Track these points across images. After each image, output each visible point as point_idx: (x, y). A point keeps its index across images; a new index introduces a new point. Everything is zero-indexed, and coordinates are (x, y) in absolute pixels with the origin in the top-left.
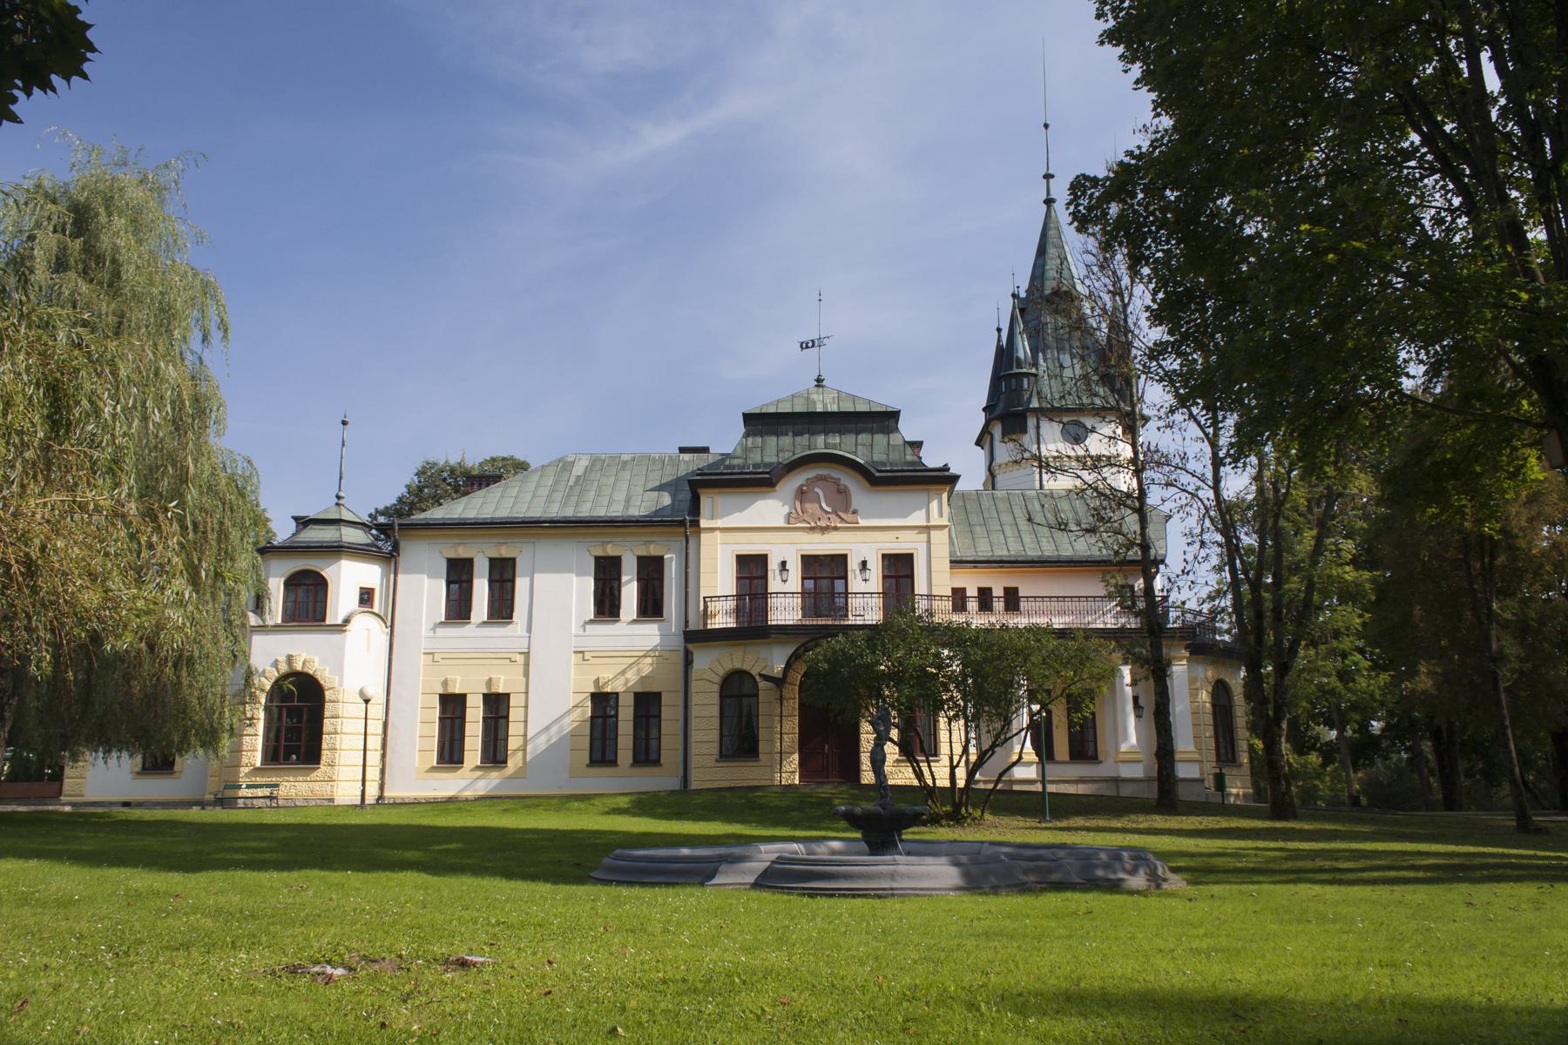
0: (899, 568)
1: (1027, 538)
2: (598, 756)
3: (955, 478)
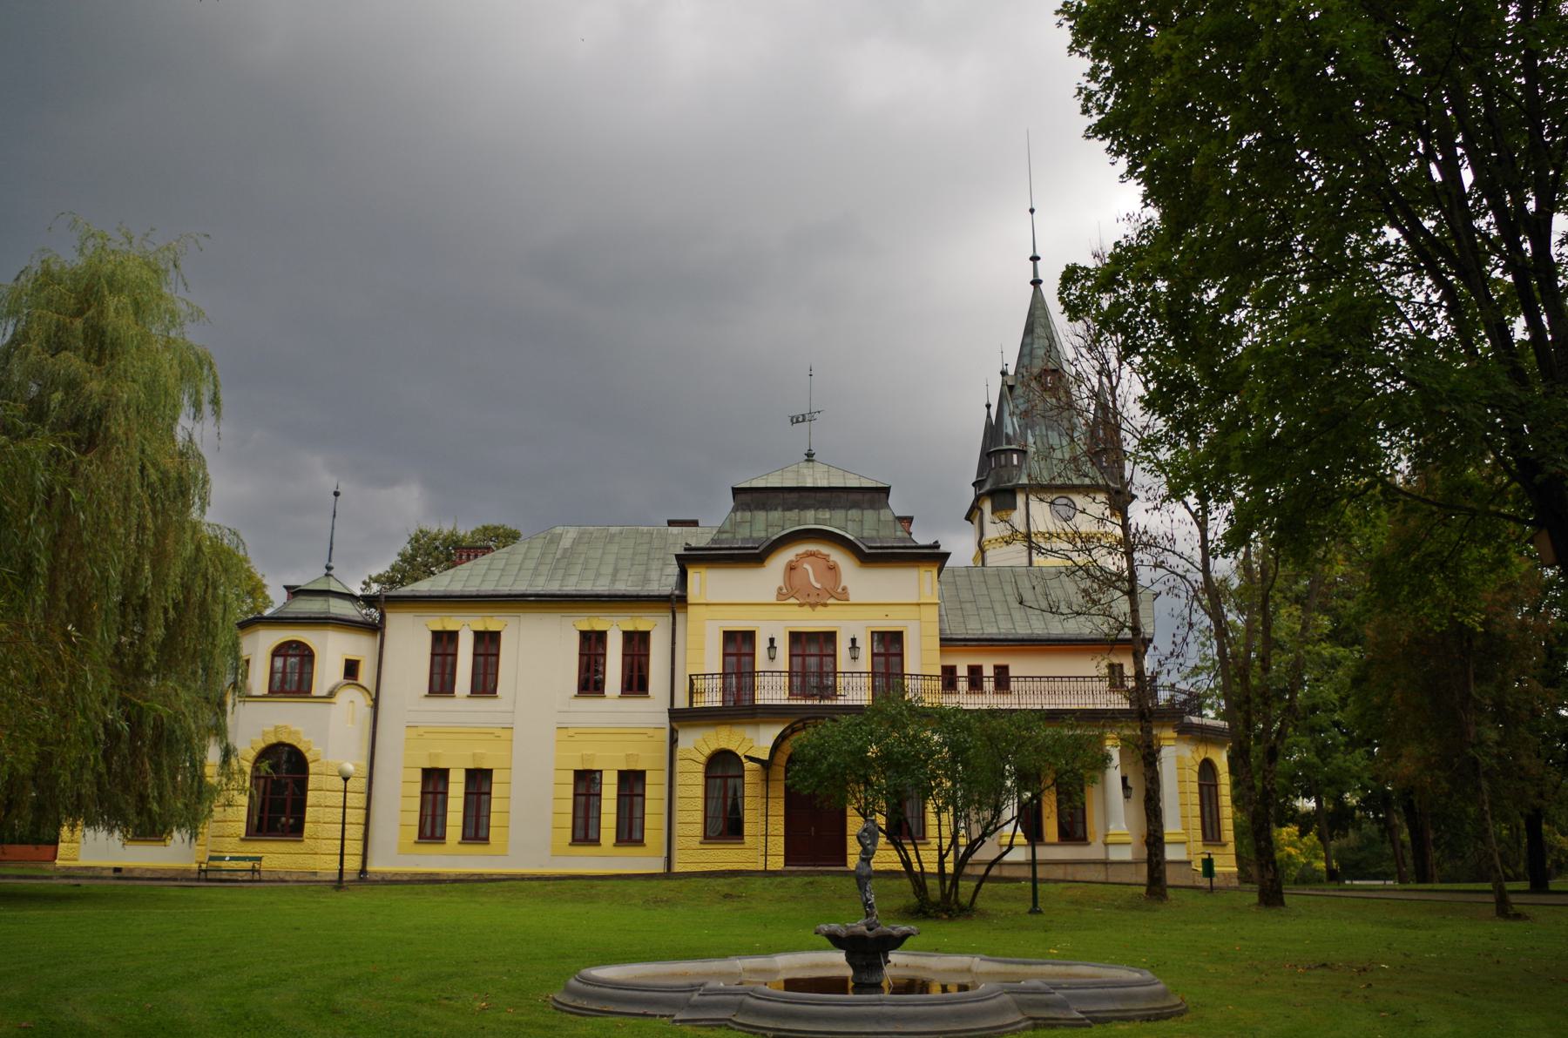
0: (889, 643)
2: (580, 834)
3: (947, 555)
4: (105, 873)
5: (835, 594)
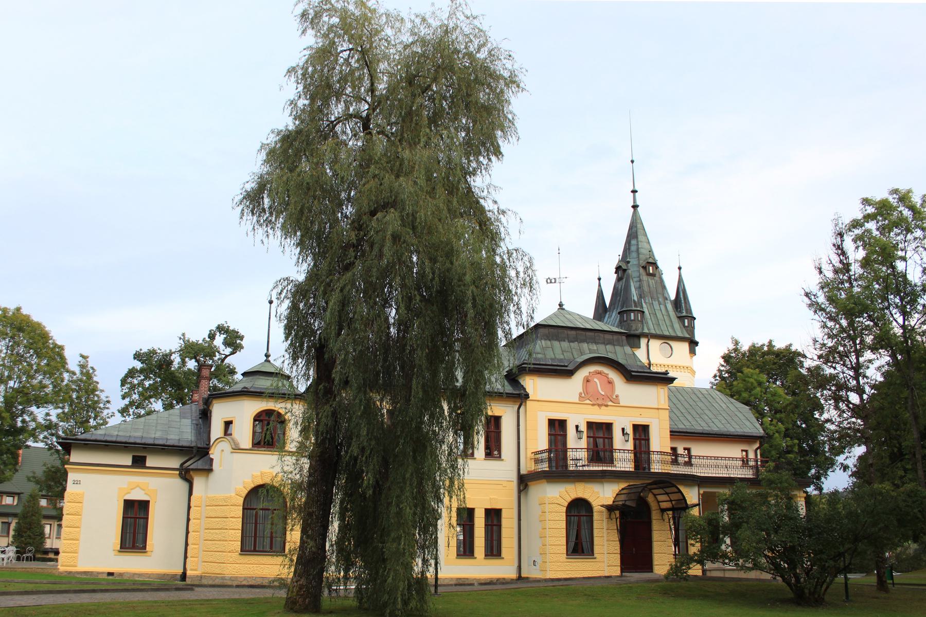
0: (641, 431)
1: (690, 418)
4: (100, 577)
5: (610, 399)
